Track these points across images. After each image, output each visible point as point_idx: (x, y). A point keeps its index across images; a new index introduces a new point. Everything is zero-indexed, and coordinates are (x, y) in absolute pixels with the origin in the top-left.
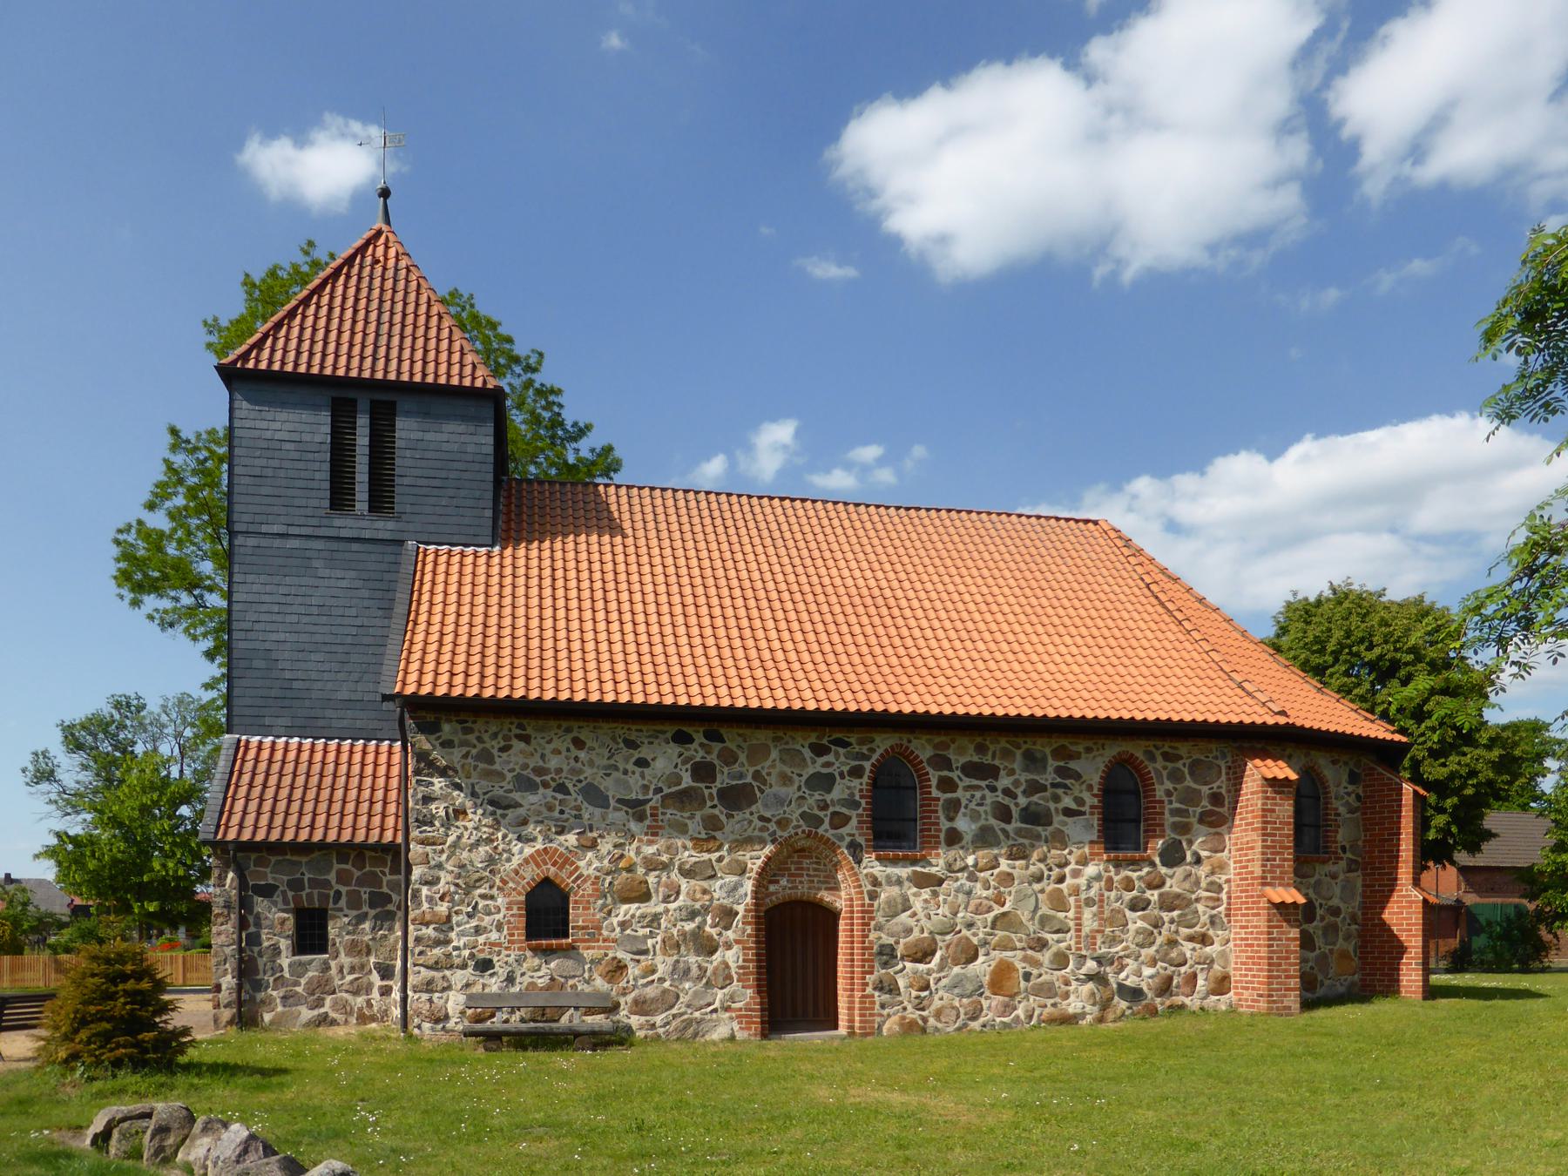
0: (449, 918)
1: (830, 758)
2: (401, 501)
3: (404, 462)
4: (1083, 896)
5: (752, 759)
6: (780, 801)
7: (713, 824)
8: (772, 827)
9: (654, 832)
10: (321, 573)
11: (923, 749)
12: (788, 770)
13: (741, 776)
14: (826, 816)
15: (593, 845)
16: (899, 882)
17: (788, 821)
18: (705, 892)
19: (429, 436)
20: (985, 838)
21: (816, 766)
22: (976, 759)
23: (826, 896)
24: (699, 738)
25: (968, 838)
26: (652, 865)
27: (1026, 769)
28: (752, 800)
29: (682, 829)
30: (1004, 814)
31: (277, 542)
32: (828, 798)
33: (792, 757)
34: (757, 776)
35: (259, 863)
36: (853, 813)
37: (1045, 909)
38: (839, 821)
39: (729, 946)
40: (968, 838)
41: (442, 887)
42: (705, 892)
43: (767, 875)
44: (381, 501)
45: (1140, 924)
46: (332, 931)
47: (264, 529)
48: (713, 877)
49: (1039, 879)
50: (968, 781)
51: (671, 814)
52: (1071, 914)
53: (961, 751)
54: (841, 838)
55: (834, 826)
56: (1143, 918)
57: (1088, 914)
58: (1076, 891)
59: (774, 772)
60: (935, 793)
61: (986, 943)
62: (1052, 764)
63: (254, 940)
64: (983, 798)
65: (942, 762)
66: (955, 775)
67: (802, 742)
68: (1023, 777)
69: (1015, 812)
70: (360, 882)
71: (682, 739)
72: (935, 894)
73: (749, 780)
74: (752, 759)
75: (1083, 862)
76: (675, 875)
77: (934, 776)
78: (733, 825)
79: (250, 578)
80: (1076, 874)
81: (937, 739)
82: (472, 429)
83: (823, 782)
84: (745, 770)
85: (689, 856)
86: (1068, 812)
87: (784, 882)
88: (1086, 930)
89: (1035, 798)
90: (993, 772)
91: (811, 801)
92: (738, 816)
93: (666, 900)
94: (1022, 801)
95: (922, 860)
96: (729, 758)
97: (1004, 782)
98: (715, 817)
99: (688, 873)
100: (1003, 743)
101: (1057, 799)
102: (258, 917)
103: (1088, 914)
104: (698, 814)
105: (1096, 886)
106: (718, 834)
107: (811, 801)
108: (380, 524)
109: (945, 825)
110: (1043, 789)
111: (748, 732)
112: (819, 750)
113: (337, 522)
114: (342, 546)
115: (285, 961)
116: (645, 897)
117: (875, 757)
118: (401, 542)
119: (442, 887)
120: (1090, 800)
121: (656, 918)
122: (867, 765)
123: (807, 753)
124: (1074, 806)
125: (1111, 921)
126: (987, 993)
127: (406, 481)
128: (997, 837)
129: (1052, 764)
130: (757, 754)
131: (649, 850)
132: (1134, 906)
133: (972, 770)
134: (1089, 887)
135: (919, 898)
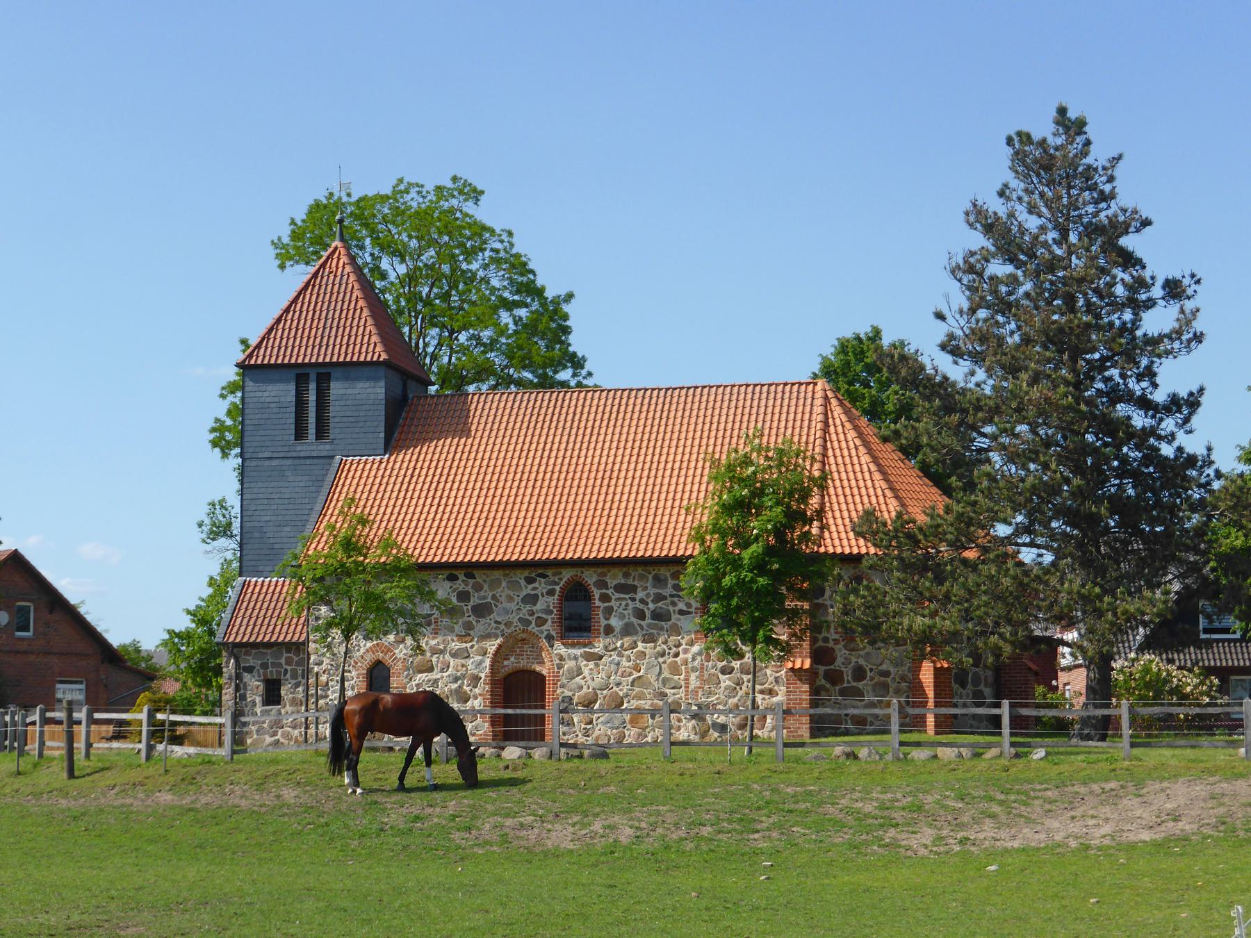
0: (327, 683)
1: (536, 585)
2: (334, 431)
3: (334, 409)
4: (690, 665)
5: (492, 588)
6: (507, 612)
7: (469, 626)
8: (502, 627)
9: (436, 633)
10: (291, 478)
11: (590, 577)
12: (511, 593)
13: (485, 598)
14: (533, 619)
15: (403, 641)
16: (576, 658)
17: (511, 623)
18: (463, 666)
19: (350, 391)
20: (628, 630)
21: (528, 590)
22: (623, 581)
23: (538, 668)
24: (462, 577)
25: (617, 630)
26: (435, 651)
27: (654, 586)
28: (491, 612)
29: (452, 630)
30: (641, 615)
31: (267, 463)
32: (534, 608)
33: (514, 585)
34: (494, 597)
35: (246, 654)
36: (549, 617)
37: (666, 674)
38: (541, 622)
39: (476, 698)
40: (617, 630)
41: (324, 666)
42: (463, 666)
43: (498, 655)
44: (321, 433)
45: (728, 683)
46: (283, 693)
47: (260, 455)
48: (468, 657)
49: (663, 655)
50: (617, 595)
51: (446, 621)
52: (682, 677)
53: (614, 577)
54: (542, 632)
55: (538, 626)
56: (729, 679)
57: (693, 676)
58: (686, 662)
59: (504, 595)
60: (598, 603)
61: (627, 695)
62: (671, 582)
63: (243, 697)
64: (627, 605)
65: (602, 584)
66: (609, 592)
67: (520, 576)
68: (652, 591)
69: (648, 614)
70: (298, 664)
71: (452, 578)
72: (597, 665)
73: (489, 600)
74: (492, 588)
75: (691, 644)
76: (447, 657)
77: (597, 593)
78: (480, 627)
79: (252, 485)
80: (686, 651)
81: (600, 570)
82: (372, 384)
83: (532, 599)
84: (487, 594)
85: (455, 645)
86: (681, 612)
87: (512, 659)
88: (692, 687)
89: (660, 604)
90: (634, 589)
91: (524, 611)
92: (483, 621)
93: (442, 671)
94: (651, 606)
95: (590, 644)
96: (478, 588)
97: (640, 595)
98: (470, 622)
99: (454, 655)
100: (640, 570)
101: (674, 604)
102: (245, 684)
103: (693, 676)
104: (461, 621)
105: (699, 658)
106: (471, 632)
107: (524, 611)
108: (321, 447)
109: (603, 622)
110: (665, 598)
111: (489, 572)
112: (530, 581)
113: (299, 448)
114: (303, 461)
115: (258, 710)
116: (431, 669)
117: (562, 582)
118: (333, 457)
119: (324, 666)
120: (695, 604)
121: (436, 681)
122: (558, 588)
123: (523, 583)
124: (685, 608)
125: (708, 681)
126: (629, 726)
127: (336, 420)
128: (635, 629)
129: (671, 582)
130: (495, 584)
131: (433, 642)
132: (723, 671)
133: (620, 588)
134: (694, 659)
135: (587, 667)
